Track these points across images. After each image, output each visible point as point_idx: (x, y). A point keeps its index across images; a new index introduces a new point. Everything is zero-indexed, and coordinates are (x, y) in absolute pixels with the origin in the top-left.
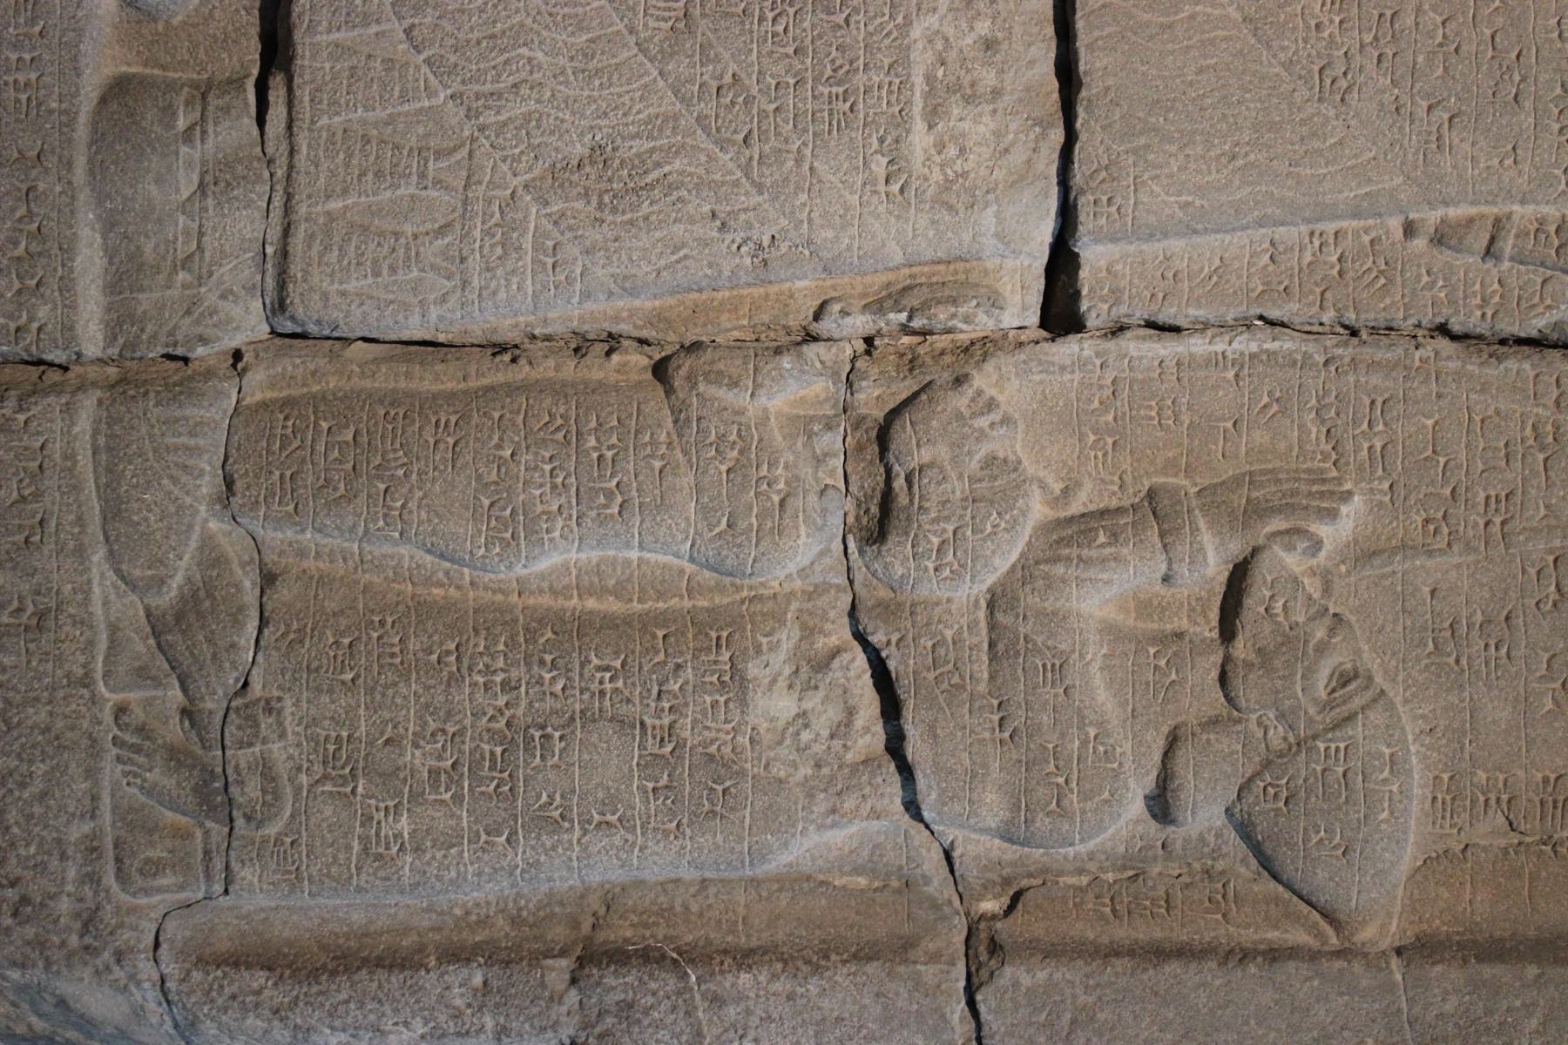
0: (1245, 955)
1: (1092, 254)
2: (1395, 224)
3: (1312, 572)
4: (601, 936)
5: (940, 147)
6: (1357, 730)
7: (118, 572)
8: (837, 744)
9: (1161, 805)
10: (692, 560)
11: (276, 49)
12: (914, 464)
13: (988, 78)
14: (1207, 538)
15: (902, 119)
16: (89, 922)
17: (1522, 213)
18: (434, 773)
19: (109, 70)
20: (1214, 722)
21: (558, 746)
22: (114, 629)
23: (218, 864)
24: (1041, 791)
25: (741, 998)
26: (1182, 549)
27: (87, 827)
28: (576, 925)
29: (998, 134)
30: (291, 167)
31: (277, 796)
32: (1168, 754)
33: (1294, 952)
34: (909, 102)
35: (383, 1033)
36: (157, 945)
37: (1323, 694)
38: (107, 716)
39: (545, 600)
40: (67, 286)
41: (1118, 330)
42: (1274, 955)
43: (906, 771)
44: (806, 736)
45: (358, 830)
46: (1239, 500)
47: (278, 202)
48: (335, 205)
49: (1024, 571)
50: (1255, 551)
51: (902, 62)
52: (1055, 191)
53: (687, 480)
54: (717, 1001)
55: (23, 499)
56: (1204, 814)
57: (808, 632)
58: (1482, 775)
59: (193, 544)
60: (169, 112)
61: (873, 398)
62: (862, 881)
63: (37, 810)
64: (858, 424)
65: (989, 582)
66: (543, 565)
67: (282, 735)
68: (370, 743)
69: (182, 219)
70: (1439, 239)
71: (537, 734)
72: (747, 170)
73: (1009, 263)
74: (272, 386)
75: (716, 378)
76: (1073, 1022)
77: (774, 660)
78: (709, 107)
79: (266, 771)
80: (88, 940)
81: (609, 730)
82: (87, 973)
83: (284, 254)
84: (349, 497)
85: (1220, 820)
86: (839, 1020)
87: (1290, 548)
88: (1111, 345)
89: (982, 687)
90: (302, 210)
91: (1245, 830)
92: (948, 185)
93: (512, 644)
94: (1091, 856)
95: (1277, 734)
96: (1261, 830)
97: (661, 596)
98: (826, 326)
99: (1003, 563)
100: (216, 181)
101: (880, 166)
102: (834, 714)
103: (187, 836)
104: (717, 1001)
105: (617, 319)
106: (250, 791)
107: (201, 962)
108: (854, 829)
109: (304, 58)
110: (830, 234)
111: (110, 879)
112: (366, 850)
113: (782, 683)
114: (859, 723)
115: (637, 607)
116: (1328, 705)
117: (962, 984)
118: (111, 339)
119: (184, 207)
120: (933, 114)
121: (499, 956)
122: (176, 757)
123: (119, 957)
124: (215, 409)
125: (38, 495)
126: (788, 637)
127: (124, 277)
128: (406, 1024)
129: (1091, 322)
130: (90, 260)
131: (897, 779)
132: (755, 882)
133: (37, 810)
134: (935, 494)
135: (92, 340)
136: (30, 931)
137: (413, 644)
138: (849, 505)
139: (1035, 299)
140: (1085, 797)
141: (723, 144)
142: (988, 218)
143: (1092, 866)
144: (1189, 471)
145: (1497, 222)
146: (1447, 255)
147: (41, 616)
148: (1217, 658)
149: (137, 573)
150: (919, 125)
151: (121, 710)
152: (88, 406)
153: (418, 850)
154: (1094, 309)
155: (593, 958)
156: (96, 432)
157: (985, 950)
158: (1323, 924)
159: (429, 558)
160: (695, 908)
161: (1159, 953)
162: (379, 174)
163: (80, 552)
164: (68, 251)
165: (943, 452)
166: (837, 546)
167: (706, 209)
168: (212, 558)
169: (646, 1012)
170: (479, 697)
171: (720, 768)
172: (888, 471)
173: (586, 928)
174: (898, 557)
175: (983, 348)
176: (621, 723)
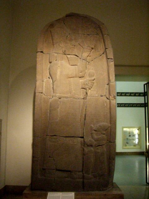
1: (80, 136)
9: (104, 134)
11: (70, 171)
17: (80, 118)
41: (84, 135)
49: (94, 139)
56: (104, 132)
61: (86, 146)
64: (87, 147)
77: (98, 151)
109: (70, 170)
126: (96, 150)
135: (82, 180)
139: (82, 138)
152: (85, 180)
154: (83, 136)
155: (110, 159)
157: (110, 142)
161: (110, 135)
174: (93, 145)
175: (84, 140)
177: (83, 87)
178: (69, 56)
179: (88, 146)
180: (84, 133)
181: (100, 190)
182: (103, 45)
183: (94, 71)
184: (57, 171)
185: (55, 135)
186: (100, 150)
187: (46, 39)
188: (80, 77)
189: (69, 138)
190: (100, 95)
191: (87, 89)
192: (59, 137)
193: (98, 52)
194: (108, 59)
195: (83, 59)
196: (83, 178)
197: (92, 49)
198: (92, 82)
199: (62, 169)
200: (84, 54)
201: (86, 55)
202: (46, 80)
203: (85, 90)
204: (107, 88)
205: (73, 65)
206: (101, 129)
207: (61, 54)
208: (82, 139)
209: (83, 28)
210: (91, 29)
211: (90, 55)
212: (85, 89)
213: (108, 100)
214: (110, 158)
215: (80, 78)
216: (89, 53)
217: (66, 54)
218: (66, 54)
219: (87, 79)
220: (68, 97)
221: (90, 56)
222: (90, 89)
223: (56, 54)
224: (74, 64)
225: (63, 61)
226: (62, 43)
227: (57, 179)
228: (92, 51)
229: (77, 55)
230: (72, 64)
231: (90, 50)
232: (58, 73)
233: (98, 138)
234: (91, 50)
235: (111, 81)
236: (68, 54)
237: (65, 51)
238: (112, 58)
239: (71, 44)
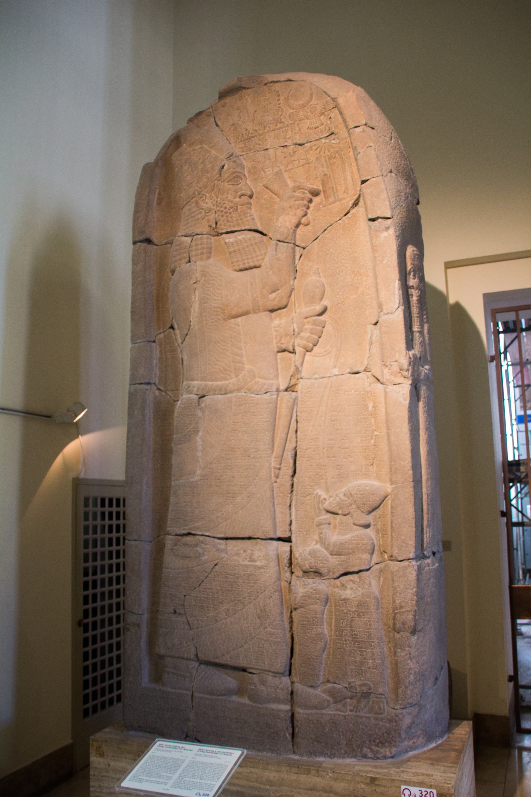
0: (392, 512)
1: (279, 534)
2: (275, 484)
3: (329, 499)
4: (391, 627)
5: (259, 560)
6: (353, 493)
7: (326, 708)
8: (356, 583)
9: (367, 526)
10: (325, 606)
12: (308, 567)
13: (249, 551)
14: (323, 517)
15: (256, 567)
16: (390, 721)
17: (273, 464)
18: (361, 655)
19: (247, 699)
20: (352, 517)
21: (356, 633)
22: (337, 710)
23: (378, 696)
24: (363, 548)
25: (400, 603)
26: (324, 522)
27: (372, 719)
28: (390, 631)
29: (258, 550)
30: (260, 669)
31: (365, 684)
32: (357, 525)
33: (391, 504)
34: (252, 565)
35: (410, 668)
36: (394, 709)
37: (347, 498)
38: (351, 713)
39: (333, 632)
40: (279, 711)
41: (290, 530)
42: (392, 507)
43: (360, 571)
44: (354, 588)
45: (371, 670)
46: (317, 511)
47: (266, 672)
48: (266, 663)
49: (327, 549)
50: (324, 509)
51: (247, 566)
52: (267, 541)
53: (311, 606)
54: (401, 607)
55: (313, 723)
57: (338, 587)
58: (364, 470)
59: (322, 694)
60: (252, 689)
61: (298, 573)
62: (381, 579)
63: (369, 728)
64: (304, 576)
65: (328, 555)
66: (326, 632)
67: (355, 682)
68: (355, 666)
69: (269, 689)
70: (277, 477)
71: (354, 636)
72: (262, 593)
73: (279, 549)
74: (297, 677)
75: (295, 600)
76: (404, 543)
78: (253, 598)
79: (362, 685)
80: (394, 721)
81: (353, 624)
82: (401, 722)
83: (274, 672)
84: (313, 665)
85: (370, 516)
86: (405, 585)
87: (324, 503)
88: (293, 532)
89: (346, 557)
90: (267, 668)
91: (370, 512)
92: (266, 560)
93: (339, 639)
94: (376, 538)
95: (354, 506)
96: (369, 509)
97: (332, 612)
98: (289, 580)
99: (326, 553)
100: (263, 682)
101: (262, 570)
102: (351, 582)
103: (374, 701)
104: (401, 607)
105: (287, 616)
106: (365, 689)
107: (397, 701)
108: (372, 580)
110: (273, 580)
111: (382, 716)
112: (375, 669)
113: (346, 592)
114: (353, 579)
115: (334, 617)
116: (349, 497)
117: (398, 562)
118: (287, 704)
119: (267, 689)
120: (254, 561)
121: (396, 646)
122: (359, 702)
123: (397, 716)
124: (299, 687)
125: (312, 720)
127: (277, 700)
128: (408, 664)
129: (289, 535)
130: (274, 706)
131: (362, 573)
132: (382, 598)
133: (369, 728)
134: (313, 564)
136: (393, 732)
137: (339, 657)
138: (317, 578)
140: (363, 540)
141: (258, 596)
142: (271, 553)
143: (378, 538)
144: (314, 519)
145: (274, 468)
146: (280, 476)
147: (333, 723)
148: (341, 516)
149: (326, 705)
150: (256, 563)
151: (351, 711)
153: (375, 659)
156: (302, 709)
158: (387, 498)
159: (325, 652)
160: (386, 610)
161: (392, 527)
162: (261, 655)
163: (322, 714)
164: (273, 710)
165: (307, 562)
166: (323, 581)
167: (268, 600)
168: (324, 691)
169: (403, 620)
170: (348, 646)
171: (360, 604)
172: (310, 572)
173: (390, 629)
174: (324, 571)
176: (352, 621)
177: (284, 347)
178: (230, 239)
179: (305, 572)
180: (291, 524)
181: (365, 756)
182: (355, 169)
183: (323, 279)
184: (203, 667)
185: (189, 534)
186: (350, 591)
187: (159, 194)
188: (272, 311)
189: (239, 542)
190: (348, 370)
191: (298, 350)
192: (201, 538)
193: (335, 202)
194: (371, 223)
195: (279, 241)
196: (292, 698)
197: (316, 194)
198: (314, 323)
199: (217, 661)
200: (281, 219)
201: (287, 224)
202: (162, 335)
203: (292, 355)
204: (374, 338)
205: (246, 269)
206: (354, 506)
207: (205, 236)
208: (285, 547)
209: (279, 125)
210: (309, 121)
211: (304, 220)
212: (290, 352)
213: (379, 385)
214: (394, 624)
215: (273, 314)
216: (300, 213)
217: (222, 234)
218: (222, 234)
219: (298, 311)
220: (231, 387)
221: (306, 225)
222: (308, 351)
223: (189, 239)
224: (247, 266)
225: (211, 261)
226: (208, 195)
227: (201, 695)
228: (312, 206)
229: (260, 229)
230: (242, 267)
231: (305, 202)
232: (196, 307)
233: (342, 544)
234: (311, 201)
235: (384, 307)
236: (227, 233)
237: (216, 223)
238: (389, 215)
239: (236, 191)
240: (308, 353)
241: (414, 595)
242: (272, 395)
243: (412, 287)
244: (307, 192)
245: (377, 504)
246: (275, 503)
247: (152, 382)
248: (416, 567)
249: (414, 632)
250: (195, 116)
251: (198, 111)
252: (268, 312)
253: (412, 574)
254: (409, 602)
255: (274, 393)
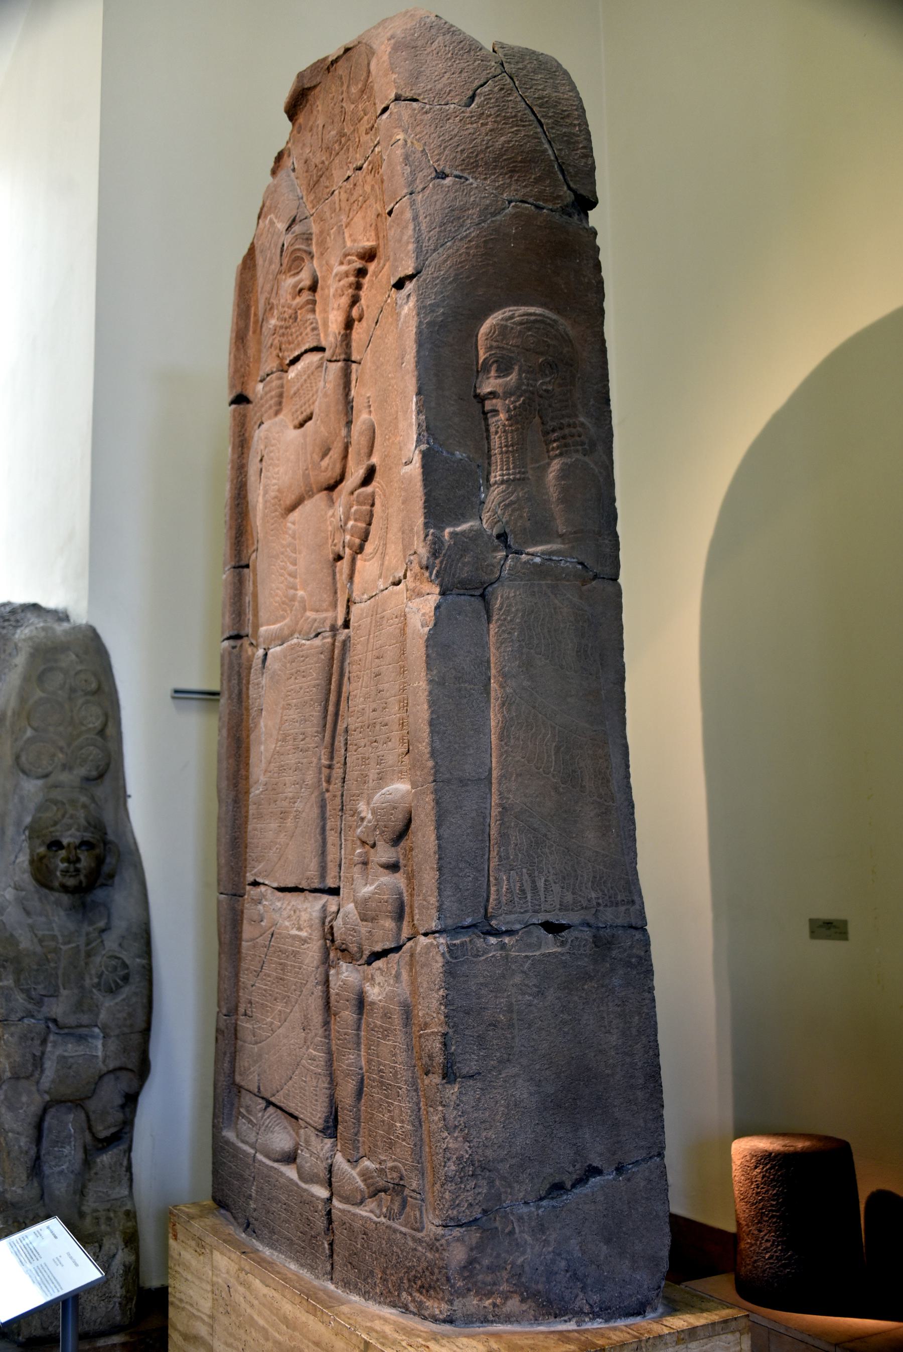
211: (355, 313)
231: (352, 279)
240: (359, 556)
241: (441, 1004)
242: (324, 638)
243: (493, 395)
244: (354, 258)
245: (400, 825)
246: (328, 828)
247: (243, 633)
248: (443, 949)
249: (449, 1075)
250: (275, 163)
251: (276, 154)
252: (325, 492)
253: (437, 962)
254: (435, 1015)
255: (327, 634)
